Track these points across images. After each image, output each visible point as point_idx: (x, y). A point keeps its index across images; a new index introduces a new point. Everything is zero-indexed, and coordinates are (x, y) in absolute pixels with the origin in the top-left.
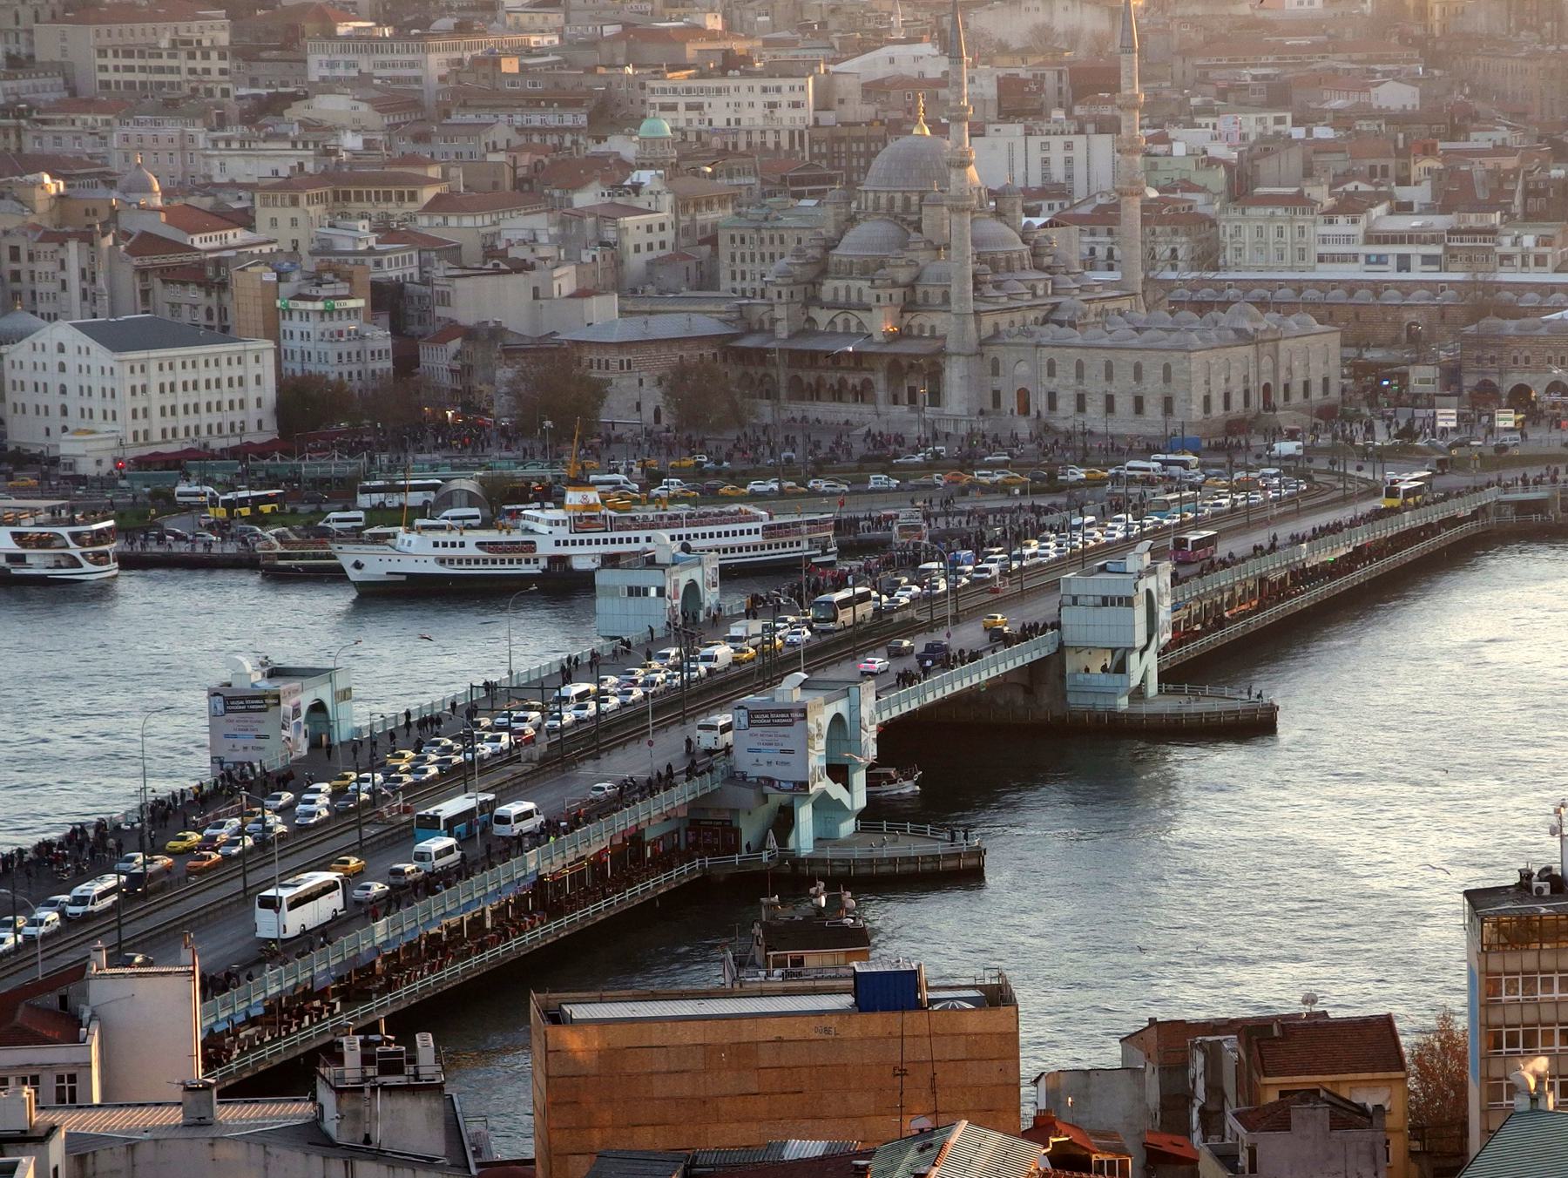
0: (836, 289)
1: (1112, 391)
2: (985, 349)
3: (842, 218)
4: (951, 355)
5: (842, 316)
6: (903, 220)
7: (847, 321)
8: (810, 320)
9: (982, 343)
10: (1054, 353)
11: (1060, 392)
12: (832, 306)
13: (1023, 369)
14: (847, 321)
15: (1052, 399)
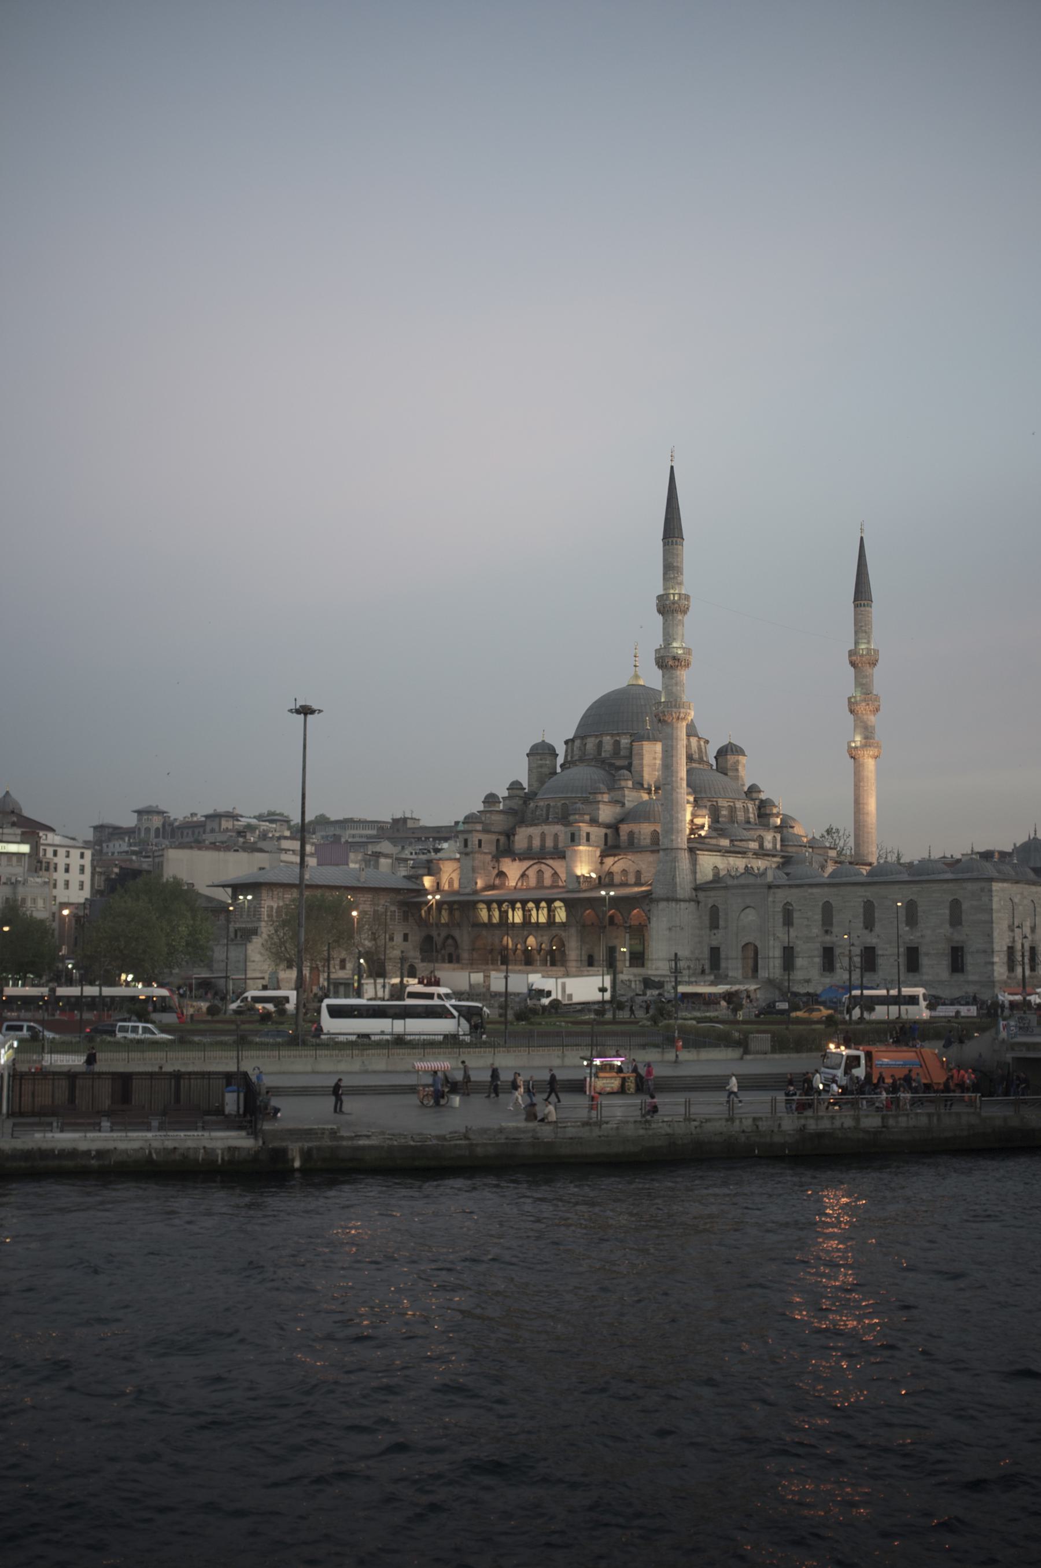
0: (530, 838)
1: (871, 940)
2: (701, 895)
3: (545, 770)
4: (658, 900)
5: (536, 867)
6: (612, 765)
7: (540, 872)
8: (501, 874)
9: (697, 888)
10: (792, 896)
11: (800, 947)
12: (523, 857)
13: (750, 917)
14: (540, 872)
15: (789, 955)
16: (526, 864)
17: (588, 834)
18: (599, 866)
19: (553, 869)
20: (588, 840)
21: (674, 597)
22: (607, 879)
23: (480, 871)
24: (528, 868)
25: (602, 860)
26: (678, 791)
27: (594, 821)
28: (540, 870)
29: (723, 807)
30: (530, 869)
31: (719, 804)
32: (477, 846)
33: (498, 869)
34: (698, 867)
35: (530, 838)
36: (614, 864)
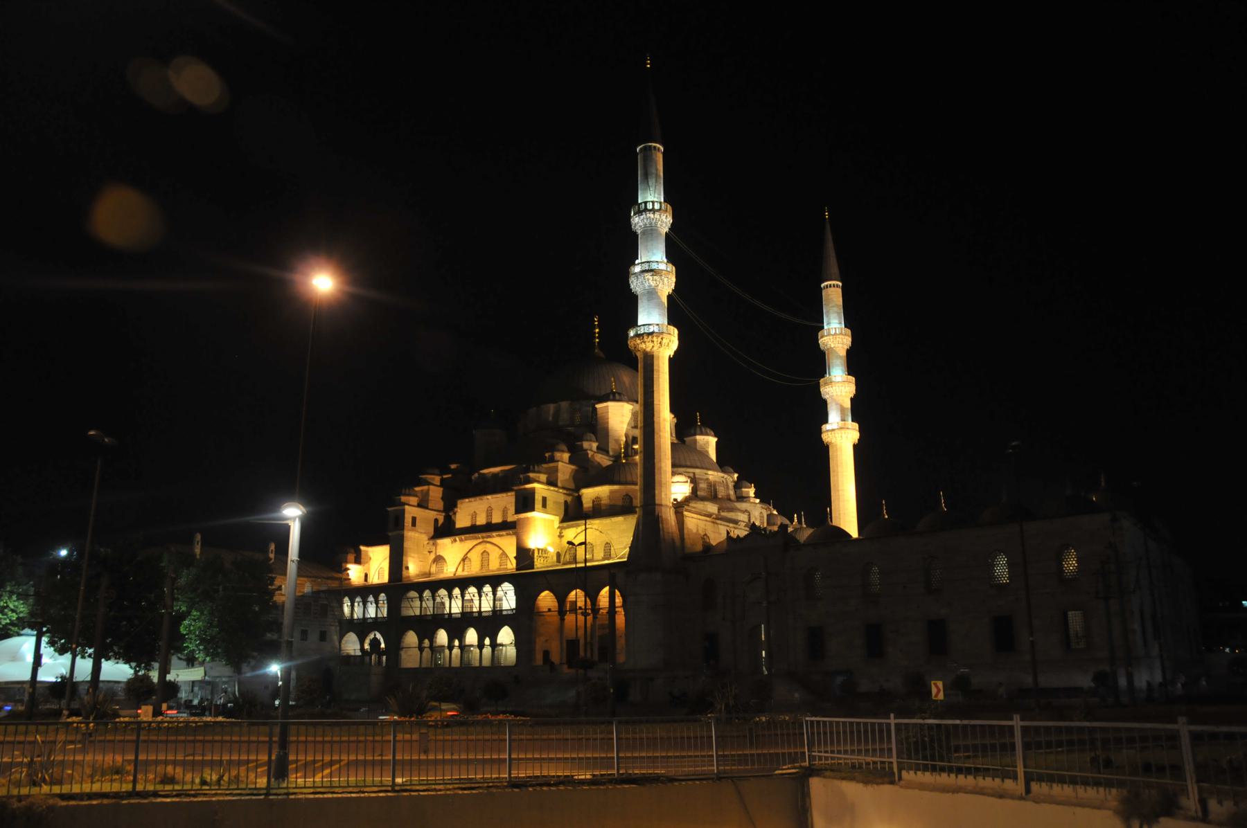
5: (480, 549)
8: (439, 559)
16: (469, 544)
17: (544, 499)
18: (557, 540)
19: (501, 549)
20: (544, 505)
21: (653, 205)
22: (568, 557)
23: (413, 555)
24: (469, 551)
25: (561, 533)
26: (662, 434)
27: (551, 482)
28: (485, 551)
29: (701, 479)
30: (473, 550)
31: (697, 476)
32: (410, 525)
33: (436, 553)
34: (685, 531)
35: (474, 516)
36: (576, 537)
